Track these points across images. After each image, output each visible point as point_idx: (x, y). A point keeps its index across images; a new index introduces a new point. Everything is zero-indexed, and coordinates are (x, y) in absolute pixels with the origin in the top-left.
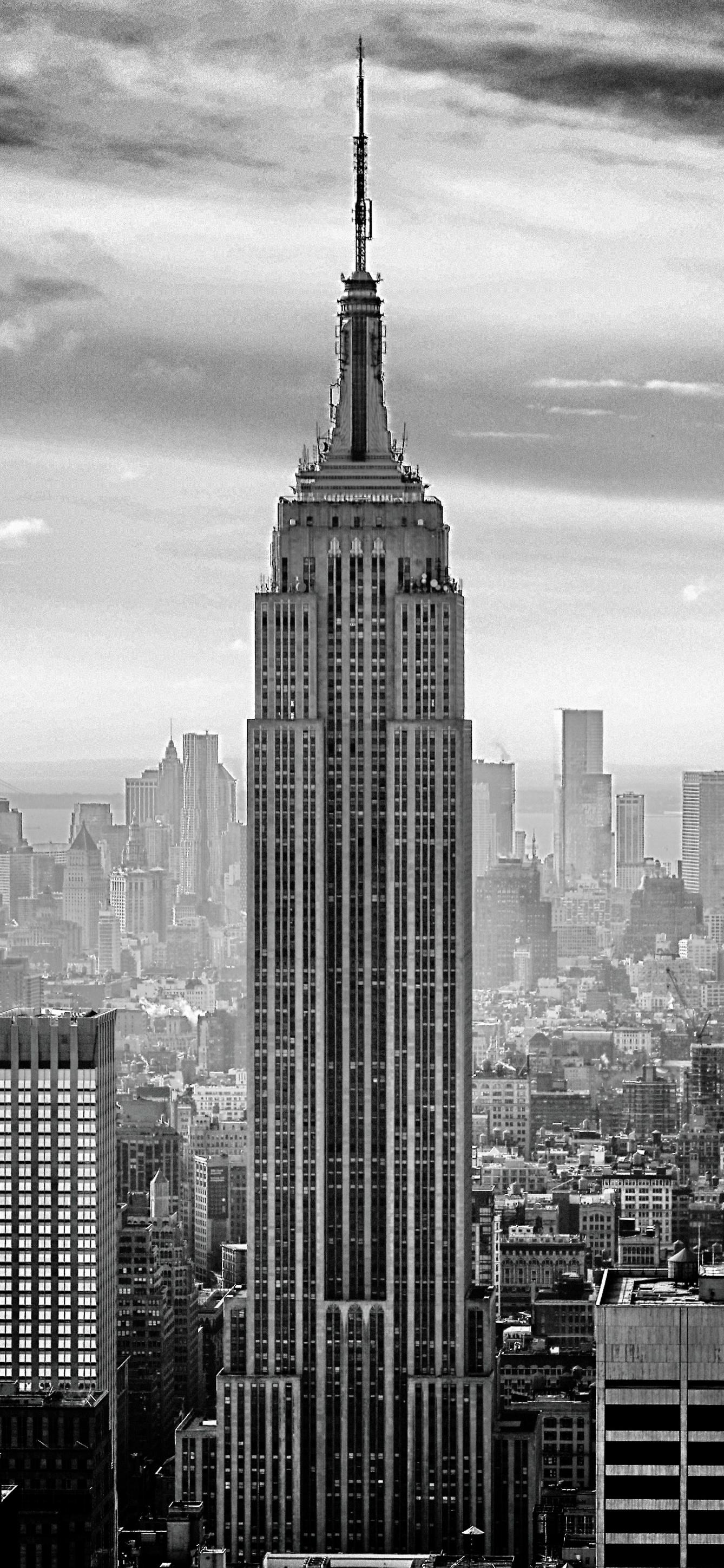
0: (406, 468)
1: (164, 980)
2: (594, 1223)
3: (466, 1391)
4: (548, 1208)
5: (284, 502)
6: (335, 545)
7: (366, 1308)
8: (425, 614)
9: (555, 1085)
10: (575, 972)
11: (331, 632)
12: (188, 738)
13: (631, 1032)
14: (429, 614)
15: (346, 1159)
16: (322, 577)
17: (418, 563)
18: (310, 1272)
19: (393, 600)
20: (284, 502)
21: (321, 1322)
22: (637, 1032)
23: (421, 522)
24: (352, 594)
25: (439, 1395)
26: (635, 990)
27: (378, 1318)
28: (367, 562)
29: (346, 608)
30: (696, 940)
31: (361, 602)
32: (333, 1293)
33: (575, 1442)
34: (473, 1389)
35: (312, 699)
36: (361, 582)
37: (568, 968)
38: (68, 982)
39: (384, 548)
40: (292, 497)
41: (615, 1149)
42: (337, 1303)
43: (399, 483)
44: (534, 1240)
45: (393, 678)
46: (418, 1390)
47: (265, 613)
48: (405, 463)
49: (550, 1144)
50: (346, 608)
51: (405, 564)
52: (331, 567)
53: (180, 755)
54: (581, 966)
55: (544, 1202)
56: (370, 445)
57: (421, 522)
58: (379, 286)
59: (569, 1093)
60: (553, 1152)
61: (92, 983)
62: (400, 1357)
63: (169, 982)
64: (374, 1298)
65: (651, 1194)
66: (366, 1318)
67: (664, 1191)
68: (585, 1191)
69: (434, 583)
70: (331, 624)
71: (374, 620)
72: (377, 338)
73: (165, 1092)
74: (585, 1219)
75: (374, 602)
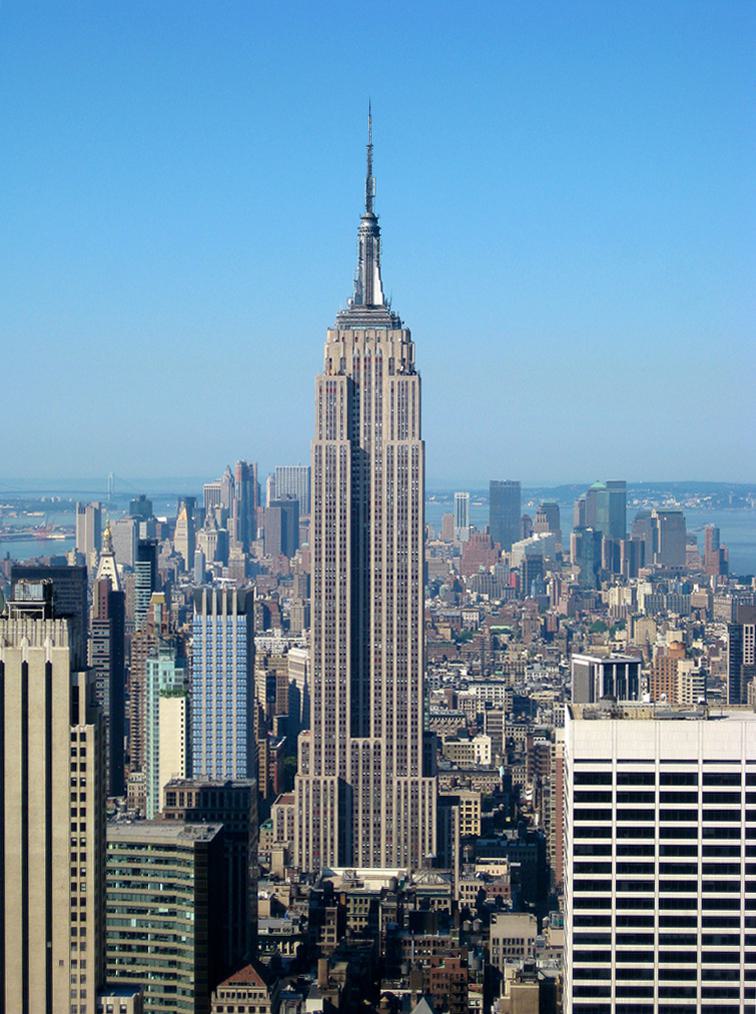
3: (424, 783)
7: (372, 741)
26: (468, 591)
27: (378, 746)
33: (473, 813)
34: (427, 784)
38: (182, 586)
42: (356, 739)
46: (399, 783)
49: (438, 667)
60: (440, 670)
62: (389, 768)
65: (493, 691)
66: (372, 747)
68: (460, 689)
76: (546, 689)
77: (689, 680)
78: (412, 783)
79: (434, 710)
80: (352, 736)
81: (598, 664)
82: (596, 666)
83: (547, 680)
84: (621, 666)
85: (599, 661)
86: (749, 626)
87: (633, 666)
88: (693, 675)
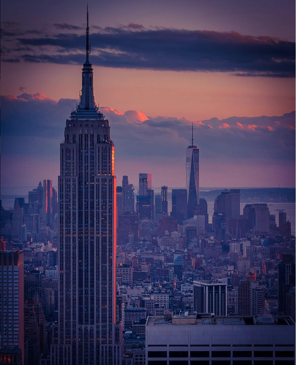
1: (38, 243)
2: (149, 305)
3: (115, 347)
4: (137, 301)
5: (67, 120)
6: (80, 131)
7: (89, 327)
9: (139, 269)
10: (145, 241)
12: (45, 181)
13: (159, 256)
15: (84, 288)
16: (77, 139)
17: (102, 136)
18: (74, 318)
19: (96, 146)
20: (67, 120)
21: (77, 331)
22: (160, 256)
23: (103, 126)
24: (85, 144)
25: (108, 349)
26: (160, 245)
27: (92, 330)
28: (89, 136)
29: (84, 147)
30: (176, 232)
32: (81, 322)
33: (143, 361)
34: (117, 347)
35: (75, 171)
36: (87, 141)
37: (143, 240)
40: (70, 119)
41: (154, 285)
42: (82, 326)
43: (97, 116)
44: (133, 309)
45: (96, 165)
46: (103, 347)
47: (63, 149)
48: (99, 111)
50: (84, 147)
51: (99, 136)
53: (43, 185)
54: (146, 239)
55: (137, 300)
56: (90, 106)
59: (143, 271)
61: (20, 244)
63: (39, 243)
64: (91, 324)
65: (163, 297)
66: (89, 330)
67: (166, 296)
69: (106, 141)
70: (80, 151)
72: (91, 79)
73: (38, 271)
74: (146, 303)
76: (190, 296)
77: (256, 293)
78: (109, 347)
79: (130, 307)
80: (79, 324)
81: (206, 286)
82: (204, 287)
83: (191, 292)
84: (217, 287)
85: (205, 284)
86: (288, 265)
87: (223, 287)
88: (258, 290)
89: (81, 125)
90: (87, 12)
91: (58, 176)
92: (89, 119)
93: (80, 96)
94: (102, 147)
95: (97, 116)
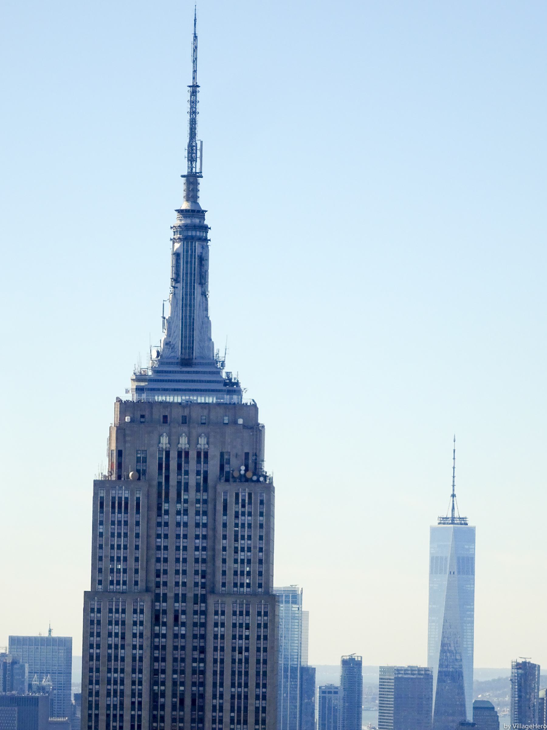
0: (228, 374)
5: (119, 400)
6: (164, 440)
8: (244, 501)
11: (159, 515)
14: (247, 501)
16: (153, 467)
17: (237, 455)
19: (215, 488)
20: (119, 400)
24: (179, 483)
28: (193, 455)
31: (186, 490)
36: (187, 473)
39: (208, 443)
40: (129, 397)
45: (214, 557)
47: (102, 498)
48: (226, 369)
51: (226, 457)
52: (160, 459)
57: (240, 421)
58: (206, 214)
71: (198, 505)
72: (203, 260)
75: (198, 490)
89: (165, 417)
90: (195, 34)
91: (85, 592)
92: (193, 398)
93: (164, 318)
94: (237, 495)
95: (221, 387)
